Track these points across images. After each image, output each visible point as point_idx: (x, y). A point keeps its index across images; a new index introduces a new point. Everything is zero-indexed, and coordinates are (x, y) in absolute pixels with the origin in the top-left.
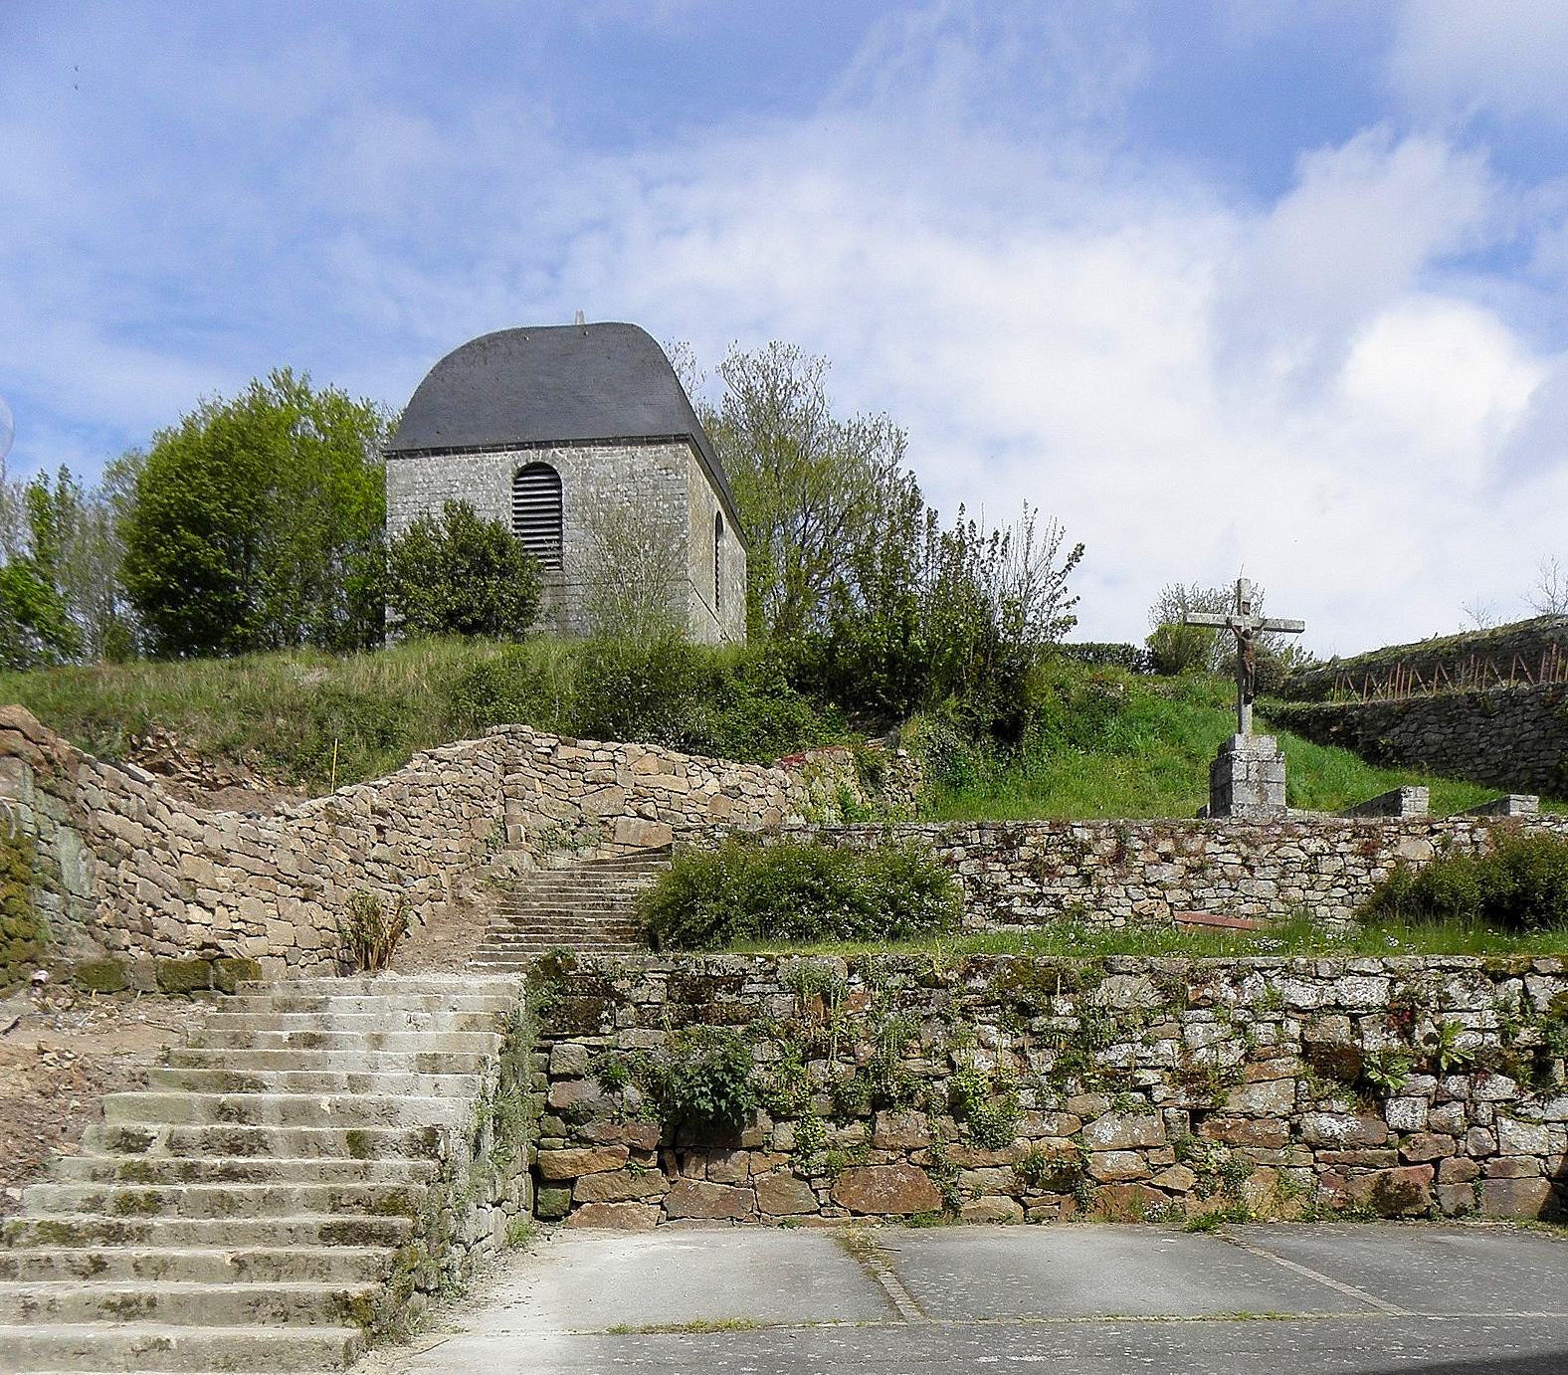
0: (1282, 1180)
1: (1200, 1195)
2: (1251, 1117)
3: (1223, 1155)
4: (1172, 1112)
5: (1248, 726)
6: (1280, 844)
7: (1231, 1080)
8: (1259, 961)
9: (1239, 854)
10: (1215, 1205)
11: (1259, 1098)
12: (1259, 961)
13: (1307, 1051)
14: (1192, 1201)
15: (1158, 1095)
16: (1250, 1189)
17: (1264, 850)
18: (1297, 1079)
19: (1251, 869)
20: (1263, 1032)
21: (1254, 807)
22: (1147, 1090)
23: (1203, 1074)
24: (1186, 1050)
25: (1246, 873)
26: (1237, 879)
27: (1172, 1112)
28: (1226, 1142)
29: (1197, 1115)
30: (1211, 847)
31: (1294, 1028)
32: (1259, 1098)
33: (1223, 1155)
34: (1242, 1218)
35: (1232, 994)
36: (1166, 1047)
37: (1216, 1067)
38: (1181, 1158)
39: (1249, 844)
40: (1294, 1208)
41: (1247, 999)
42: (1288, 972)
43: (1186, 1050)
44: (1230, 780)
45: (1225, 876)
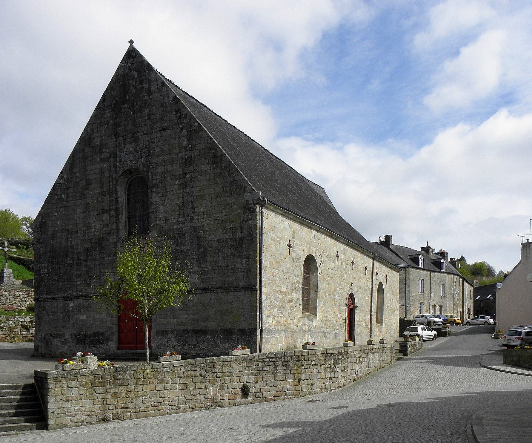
0: (19, 338)
1: (11, 339)
2: (16, 332)
3: (13, 335)
4: (8, 331)
5: (7, 267)
6: (14, 292)
7: (14, 328)
8: (16, 316)
9: (8, 293)
10: (12, 340)
11: (17, 330)
12: (16, 316)
13: (22, 325)
14: (10, 340)
15: (6, 329)
16: (16, 339)
17: (12, 293)
18: (21, 328)
19: (10, 296)
20: (17, 323)
21: (8, 281)
22: (5, 329)
23: (11, 327)
24: (9, 325)
25: (9, 296)
26: (8, 297)
27: (8, 331)
28: (13, 334)
29: (10, 331)
30: (3, 292)
31: (20, 323)
32: (17, 330)
33: (13, 335)
34: (15, 342)
35: (14, 320)
36: (7, 325)
37: (12, 327)
38: (9, 336)
39: (10, 292)
40: (20, 341)
41: (15, 320)
42: (20, 317)
43: (9, 325)
44: (4, 276)
45: (6, 297)
